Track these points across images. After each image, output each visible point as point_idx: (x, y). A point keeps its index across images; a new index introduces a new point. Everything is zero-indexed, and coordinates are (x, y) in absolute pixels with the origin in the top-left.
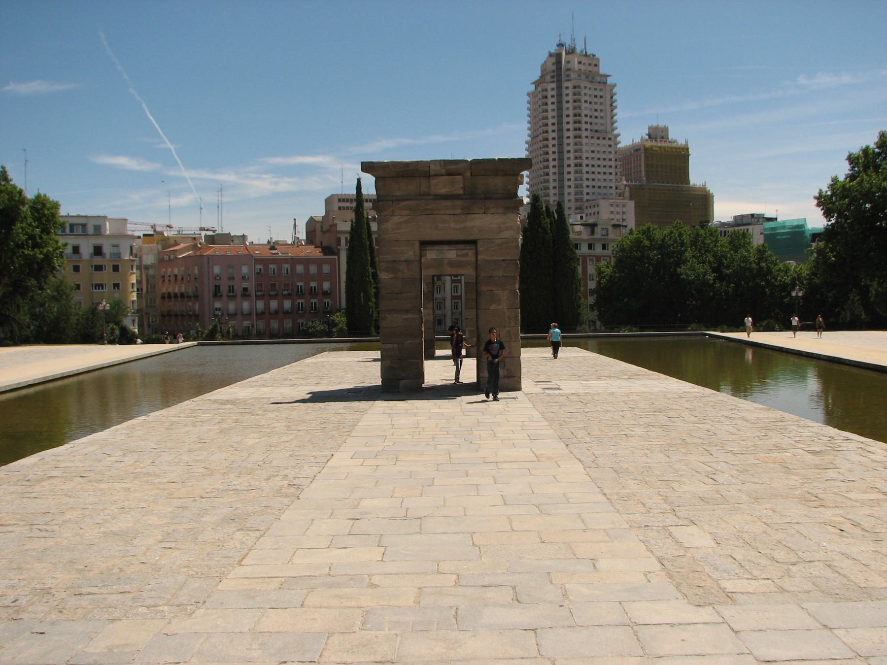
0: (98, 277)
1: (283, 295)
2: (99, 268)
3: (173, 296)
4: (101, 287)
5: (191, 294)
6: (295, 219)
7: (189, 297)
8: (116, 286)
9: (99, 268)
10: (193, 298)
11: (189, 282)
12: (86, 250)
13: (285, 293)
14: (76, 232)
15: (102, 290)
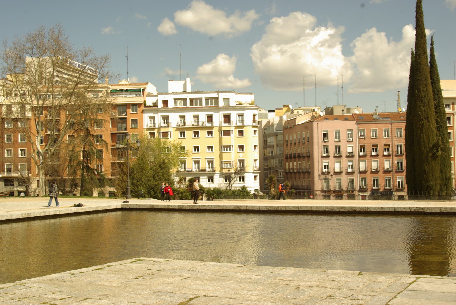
0: (226, 141)
1: (384, 156)
2: (227, 133)
3: (293, 156)
4: (228, 148)
5: (305, 155)
6: (398, 91)
7: (304, 157)
8: (241, 147)
9: (227, 133)
10: (306, 158)
11: (304, 143)
12: (218, 118)
13: (386, 153)
14: (211, 105)
15: (230, 151)
